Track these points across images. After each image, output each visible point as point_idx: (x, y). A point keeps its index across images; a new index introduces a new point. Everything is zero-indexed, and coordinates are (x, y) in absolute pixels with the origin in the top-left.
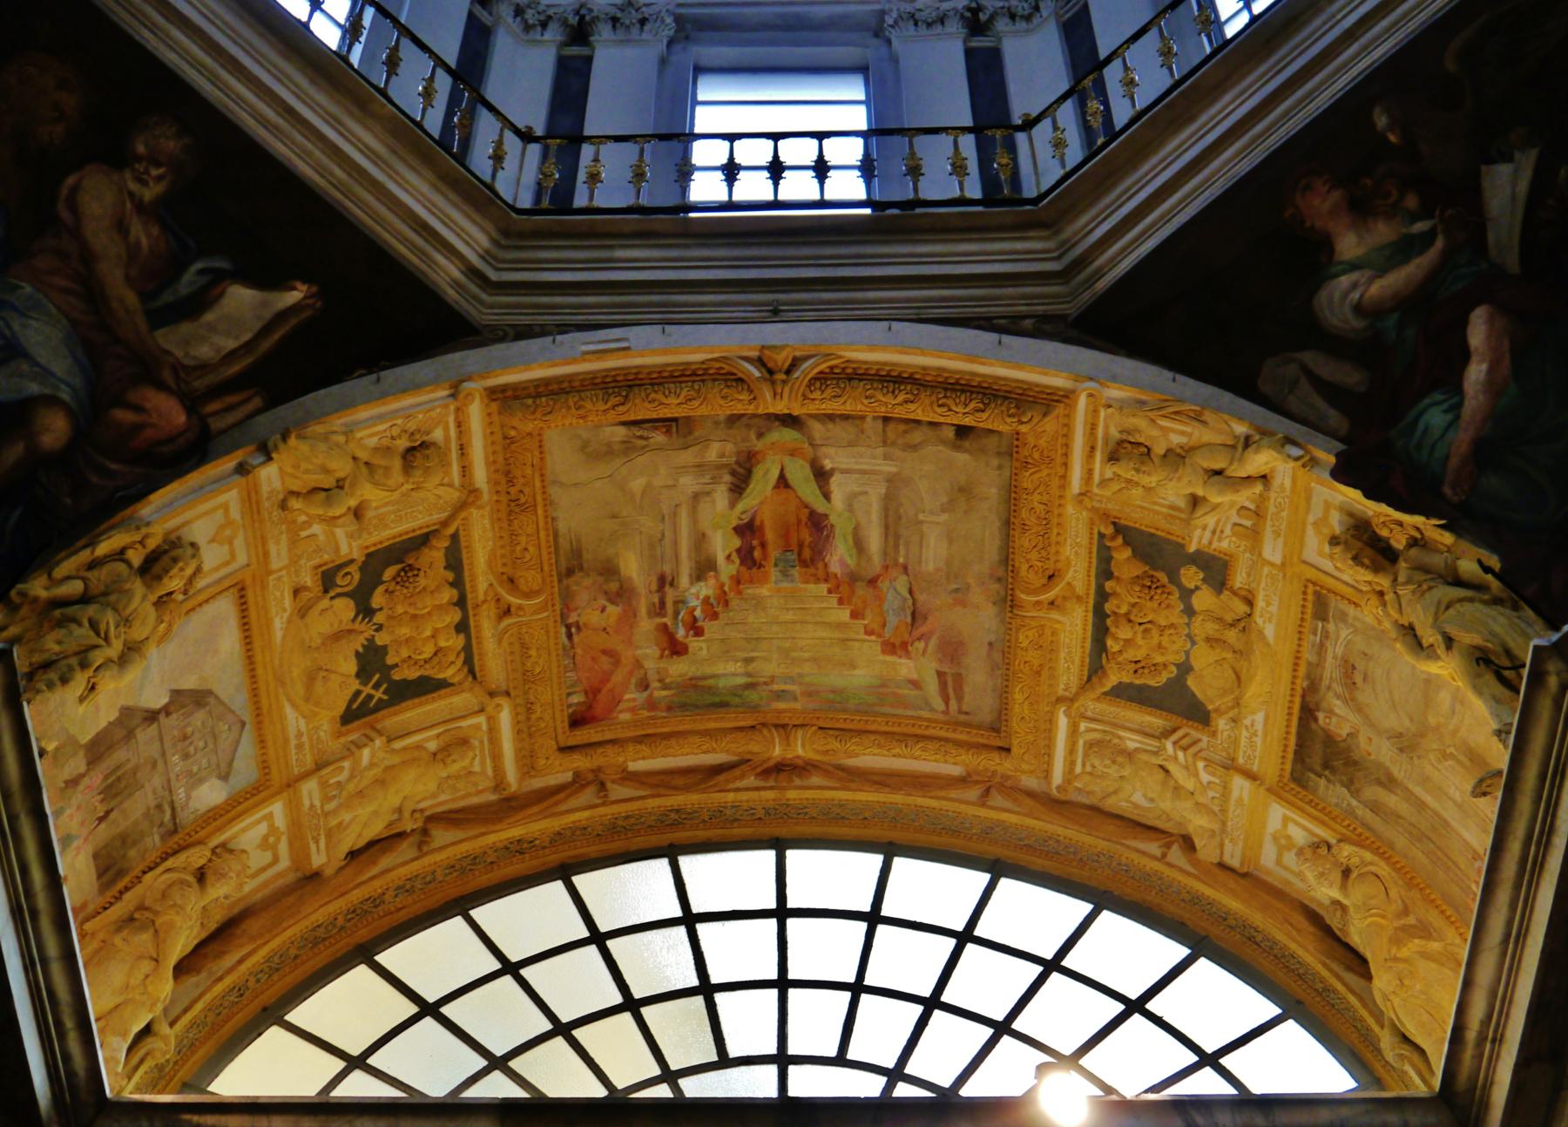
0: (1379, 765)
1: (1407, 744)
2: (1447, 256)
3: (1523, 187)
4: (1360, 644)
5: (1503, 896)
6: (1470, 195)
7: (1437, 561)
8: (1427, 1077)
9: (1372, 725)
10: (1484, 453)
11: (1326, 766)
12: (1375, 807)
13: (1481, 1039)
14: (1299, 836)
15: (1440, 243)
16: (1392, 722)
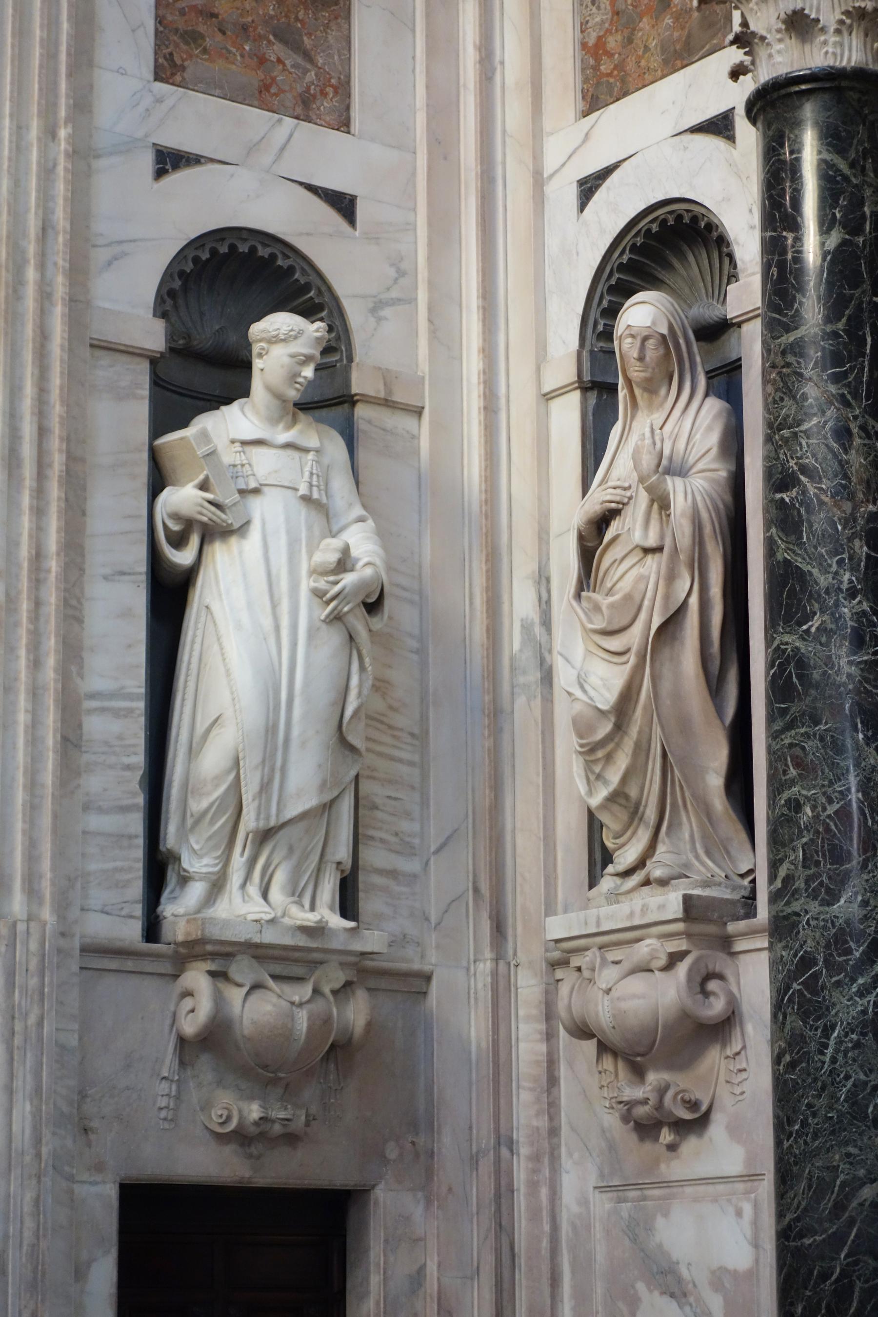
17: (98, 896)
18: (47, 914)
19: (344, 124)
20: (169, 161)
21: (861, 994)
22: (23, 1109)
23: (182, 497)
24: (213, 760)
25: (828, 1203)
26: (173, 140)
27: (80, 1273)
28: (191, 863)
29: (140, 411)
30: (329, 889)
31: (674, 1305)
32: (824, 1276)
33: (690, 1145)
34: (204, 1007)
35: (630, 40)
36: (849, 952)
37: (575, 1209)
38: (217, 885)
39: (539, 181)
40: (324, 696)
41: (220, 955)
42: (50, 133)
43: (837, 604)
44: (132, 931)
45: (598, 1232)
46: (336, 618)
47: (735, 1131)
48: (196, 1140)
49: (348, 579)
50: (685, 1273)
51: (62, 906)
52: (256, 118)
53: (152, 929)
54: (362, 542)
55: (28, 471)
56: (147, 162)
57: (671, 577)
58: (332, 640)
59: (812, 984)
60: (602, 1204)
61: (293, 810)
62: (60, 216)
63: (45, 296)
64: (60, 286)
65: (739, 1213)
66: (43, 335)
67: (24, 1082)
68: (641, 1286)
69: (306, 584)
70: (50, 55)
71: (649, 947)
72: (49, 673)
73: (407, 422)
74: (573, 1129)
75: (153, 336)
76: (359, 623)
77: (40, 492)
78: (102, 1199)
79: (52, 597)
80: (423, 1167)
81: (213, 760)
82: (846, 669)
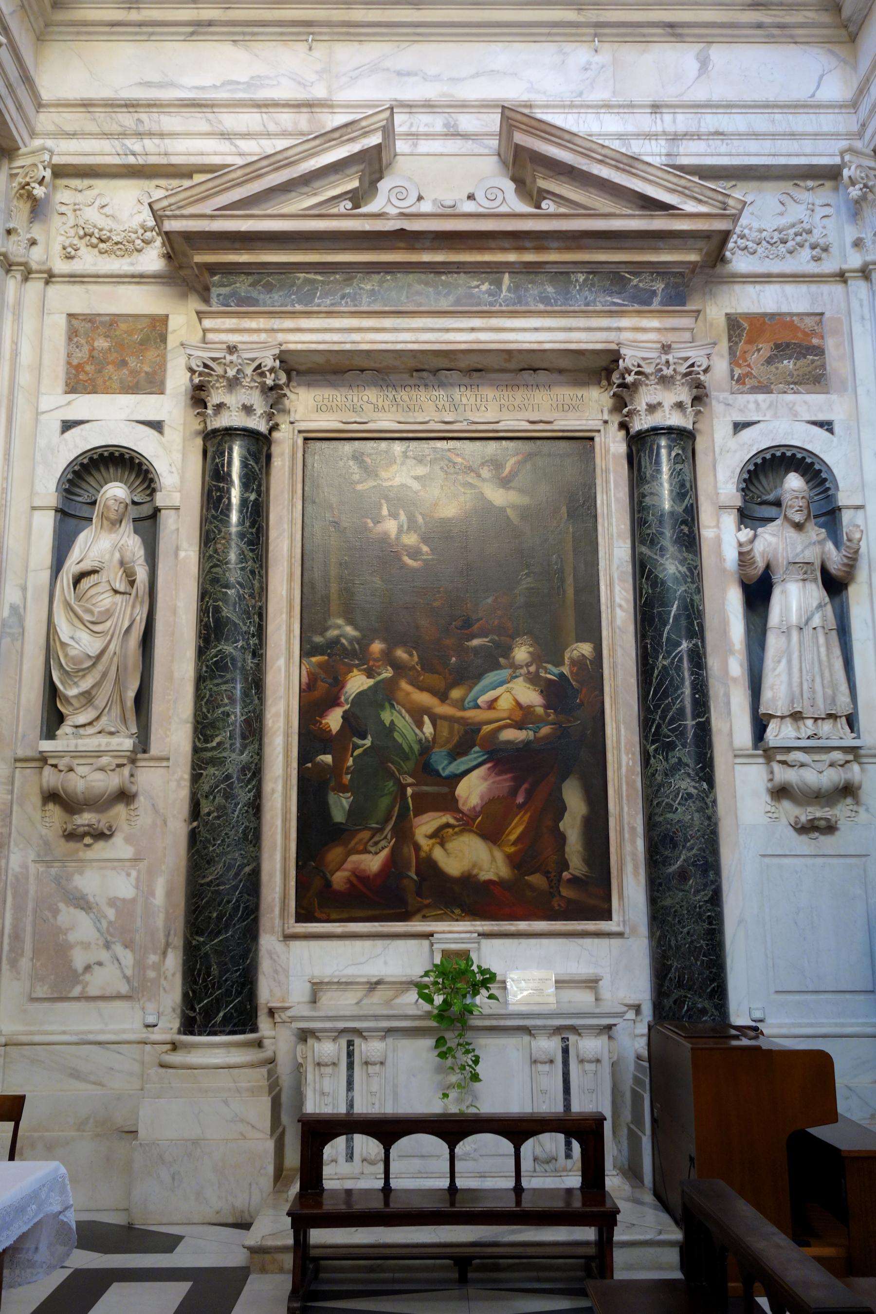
21: (249, 792)
25: (232, 873)
31: (83, 913)
32: (229, 902)
33: (101, 844)
35: (100, 371)
36: (246, 775)
37: (17, 869)
43: (248, 639)
45: (32, 879)
47: (128, 840)
50: (91, 899)
59: (231, 786)
60: (32, 868)
65: (128, 875)
68: (61, 905)
74: (19, 833)
82: (251, 665)
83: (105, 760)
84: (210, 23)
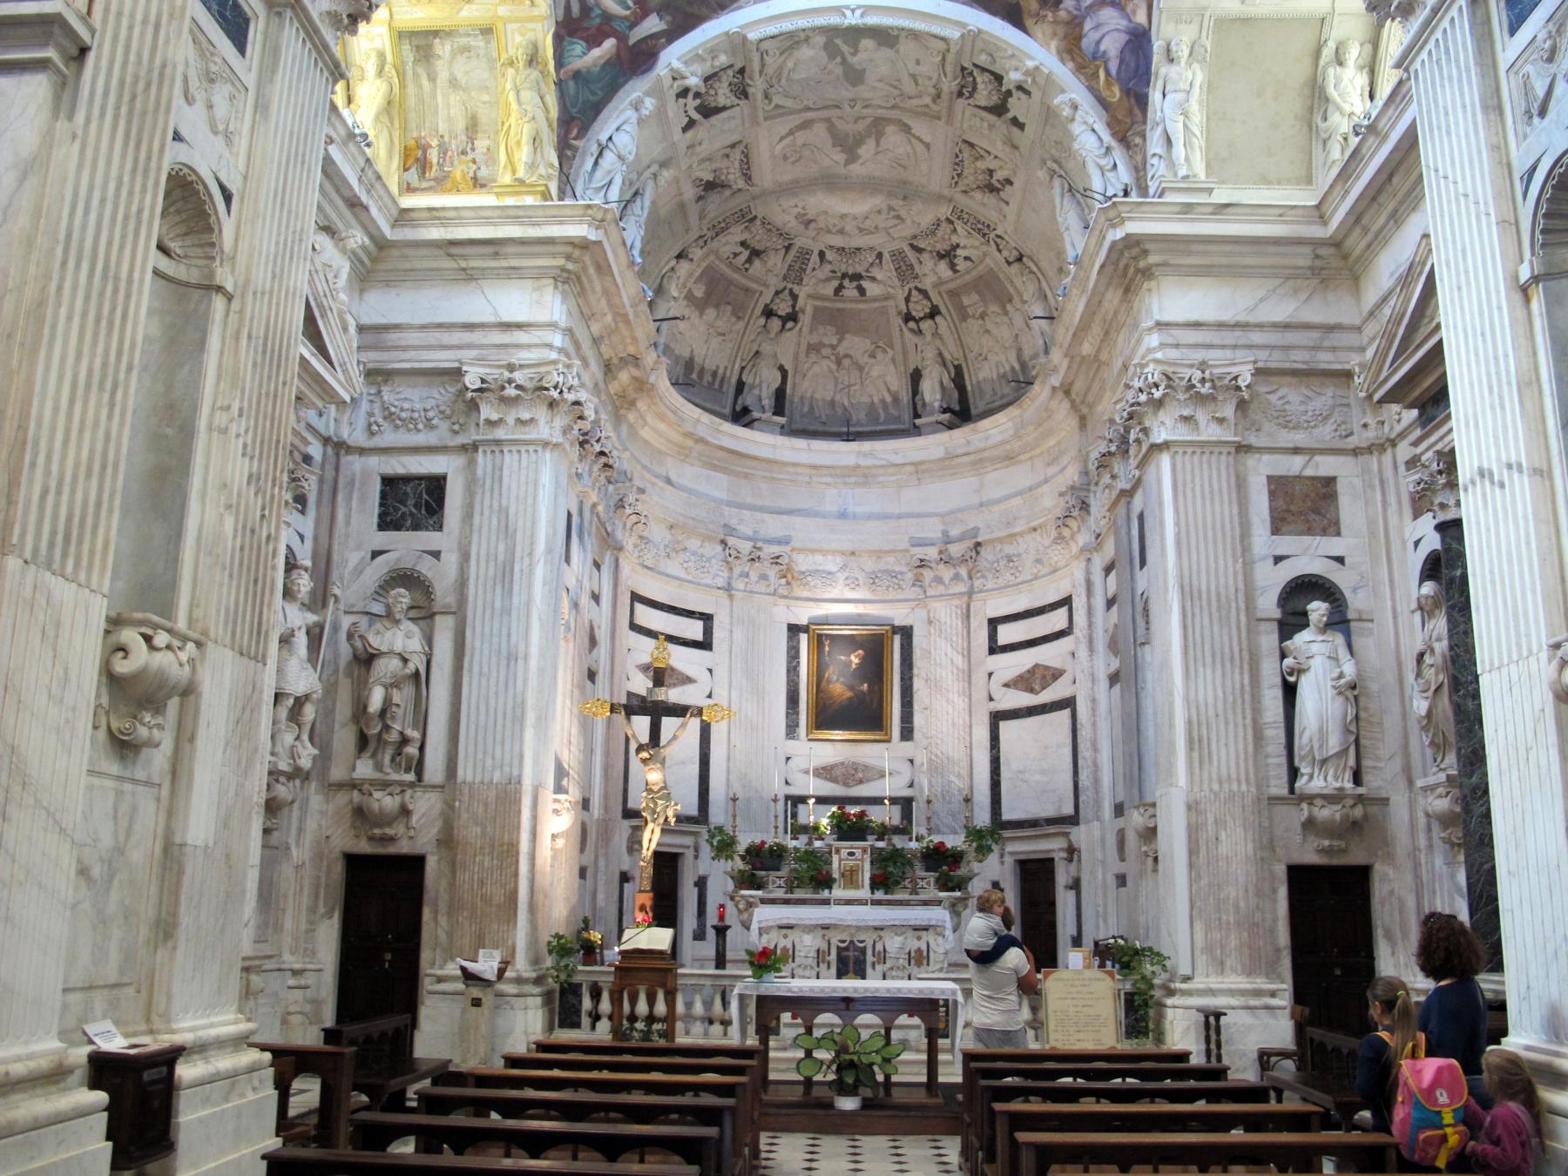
0: (435, 72)
1: (453, 83)
2: (626, 18)
3: (655, 30)
4: (482, 52)
5: (498, 213)
6: (645, 14)
7: (544, 88)
8: (196, 30)
9: (451, 63)
10: (577, 75)
11: (418, 47)
12: (415, 75)
13: (439, 218)
14: (378, 44)
15: (628, 13)
16: (459, 76)
17: (1273, 782)
18: (1253, 789)
19: (1338, 534)
20: (1278, 559)
22: (1250, 846)
23: (1288, 662)
24: (1305, 739)
26: (1279, 552)
27: (1274, 891)
28: (1303, 770)
29: (1275, 636)
30: (1348, 775)
34: (1306, 813)
38: (1311, 776)
39: (1404, 542)
40: (1338, 714)
41: (1310, 799)
42: (1235, 561)
44: (1285, 792)
46: (1340, 693)
48: (1309, 854)
49: (1343, 681)
51: (1258, 786)
52: (1307, 539)
53: (1292, 790)
54: (1349, 669)
55: (1237, 662)
56: (1271, 560)
57: (1437, 674)
58: (1340, 699)
60: (1445, 868)
61: (1331, 752)
62: (1241, 586)
63: (1238, 610)
64: (1242, 606)
66: (1238, 621)
67: (1250, 837)
69: (1330, 684)
70: (1233, 538)
71: (1441, 790)
72: (1249, 721)
73: (1370, 625)
75: (1277, 614)
76: (1349, 694)
77: (1241, 667)
78: (1281, 871)
79: (1247, 697)
80: (1390, 857)
81: (1305, 739)
83: (1441, 790)
84: (1395, 211)
